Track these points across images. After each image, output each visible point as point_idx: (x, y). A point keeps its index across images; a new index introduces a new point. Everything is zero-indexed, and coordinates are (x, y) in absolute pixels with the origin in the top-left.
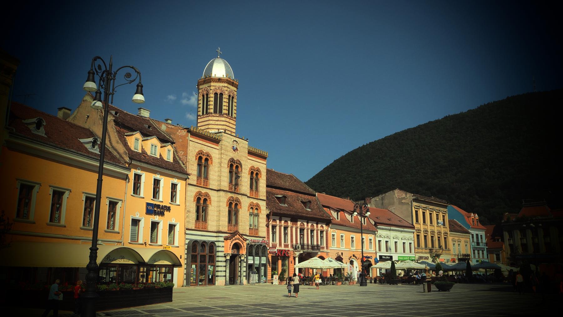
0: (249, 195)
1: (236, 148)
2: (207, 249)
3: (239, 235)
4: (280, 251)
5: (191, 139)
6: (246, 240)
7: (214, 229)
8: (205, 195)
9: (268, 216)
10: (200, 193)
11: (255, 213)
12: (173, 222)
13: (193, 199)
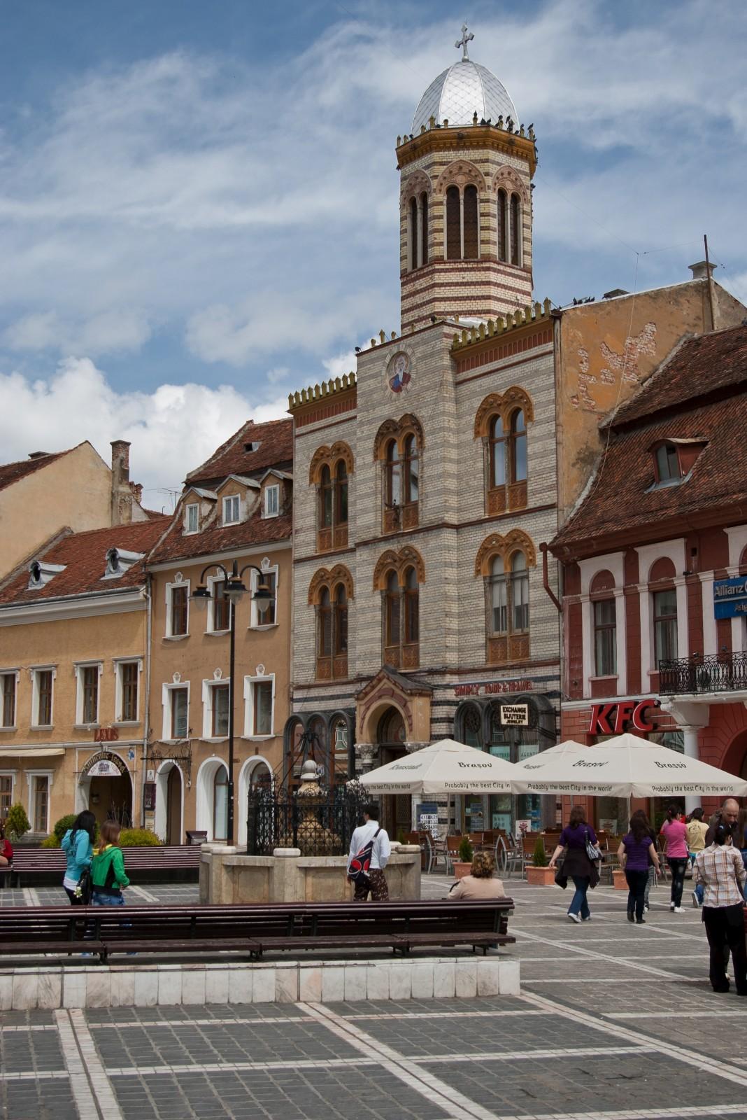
1: (405, 374)
10: (320, 576)
13: (306, 598)
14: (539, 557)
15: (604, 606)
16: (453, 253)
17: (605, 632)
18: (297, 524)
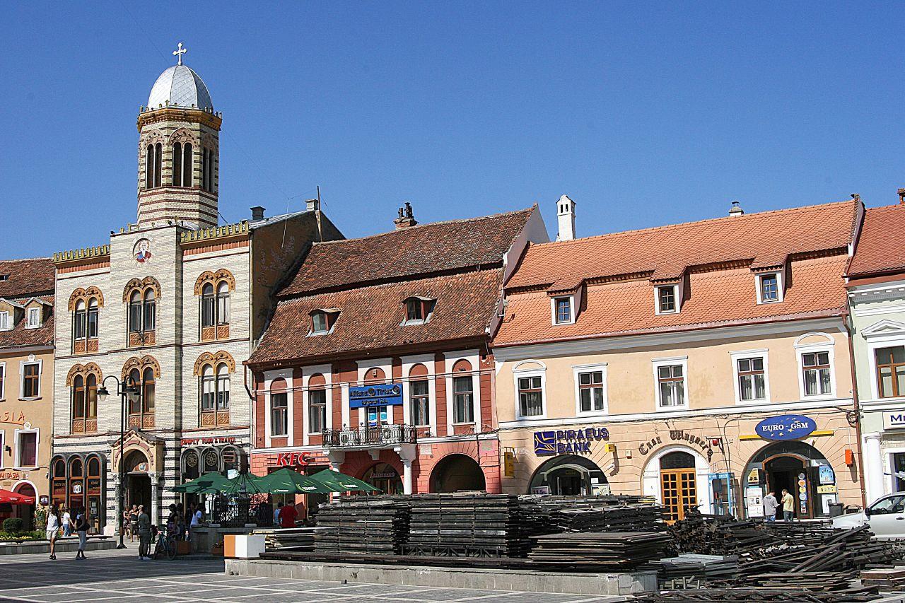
2: (85, 468)
5: (59, 276)
10: (78, 368)
12: (27, 430)
14: (240, 368)
16: (176, 183)
18: (58, 334)
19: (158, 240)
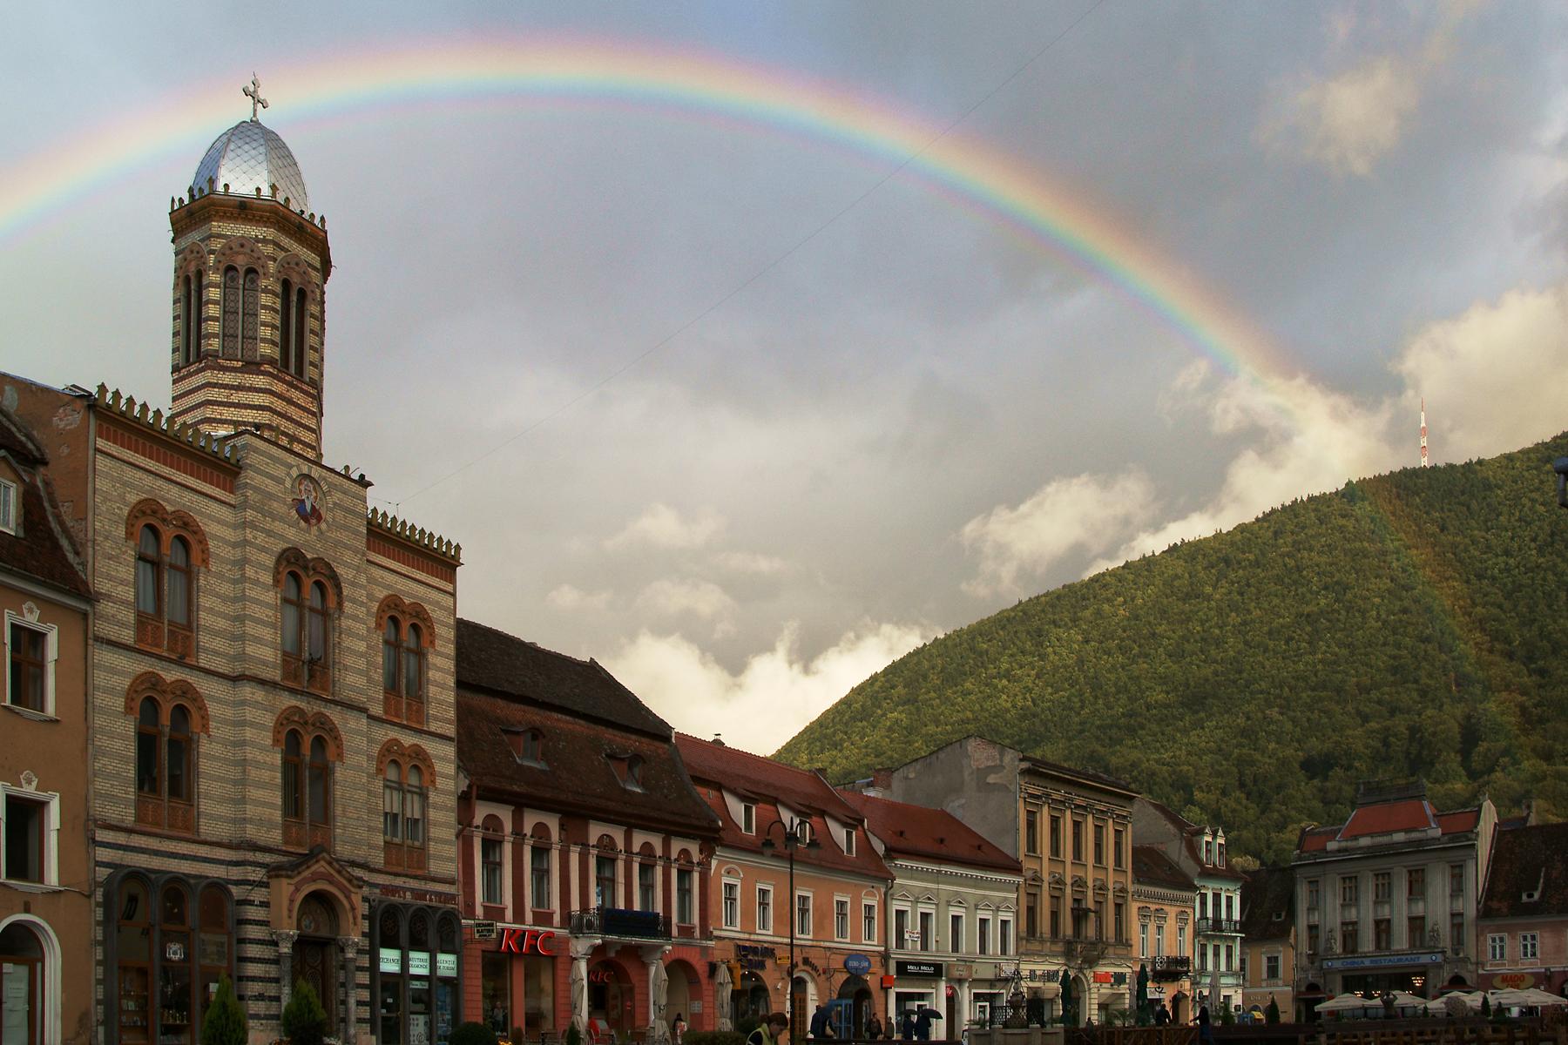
0: (377, 710)
1: (313, 507)
3: (330, 864)
4: (519, 936)
6: (361, 883)
7: (223, 831)
8: (178, 692)
9: (465, 801)
11: (409, 785)
15: (491, 846)
17: (492, 868)
19: (337, 496)
